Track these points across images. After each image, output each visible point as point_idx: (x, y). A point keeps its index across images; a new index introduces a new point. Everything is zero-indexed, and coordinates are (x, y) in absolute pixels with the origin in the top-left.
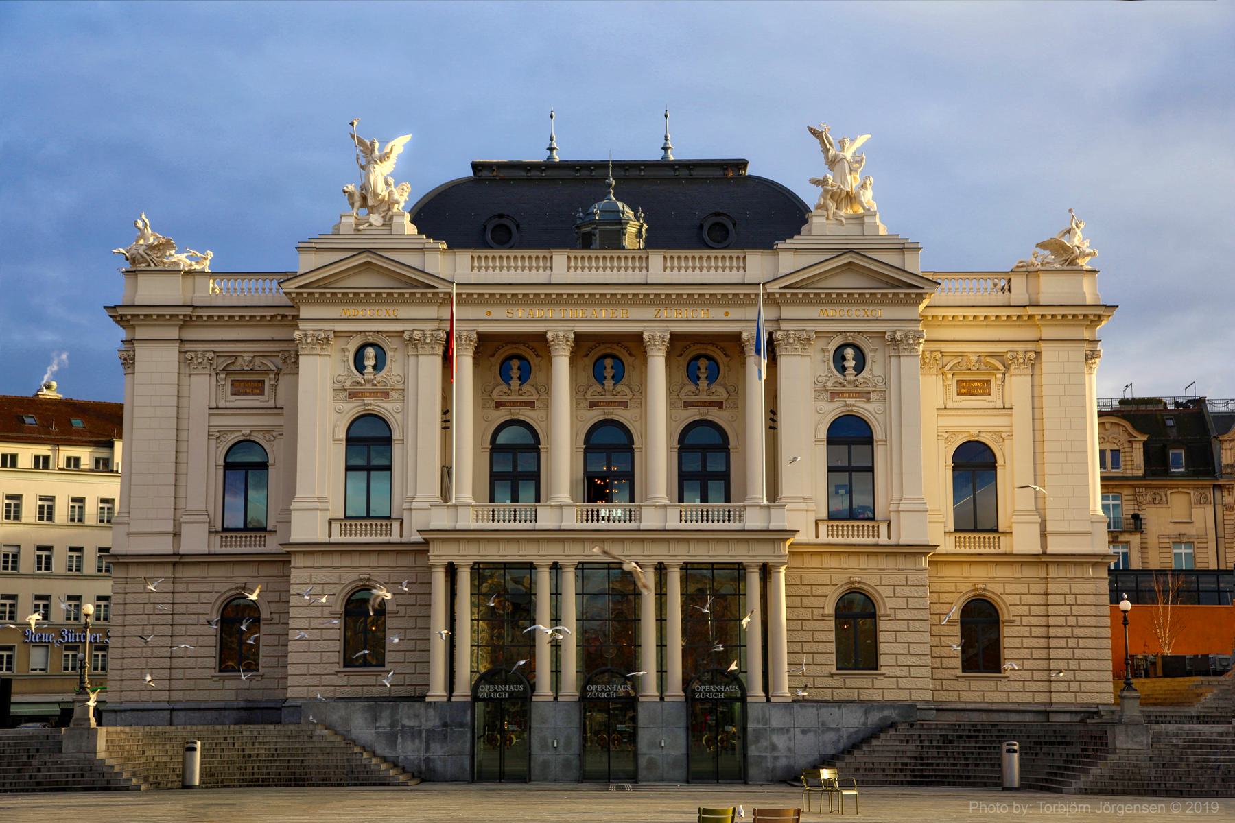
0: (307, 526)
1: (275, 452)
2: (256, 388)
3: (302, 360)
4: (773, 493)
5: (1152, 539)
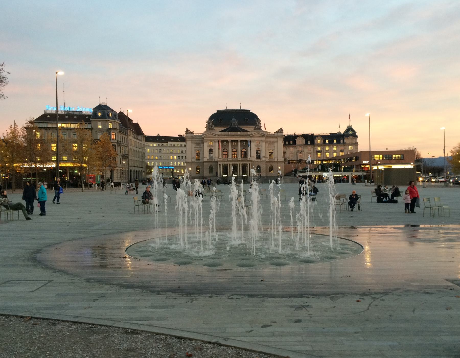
0: (205, 160)
1: (201, 152)
2: (199, 145)
3: (205, 144)
4: (251, 156)
5: (305, 153)
